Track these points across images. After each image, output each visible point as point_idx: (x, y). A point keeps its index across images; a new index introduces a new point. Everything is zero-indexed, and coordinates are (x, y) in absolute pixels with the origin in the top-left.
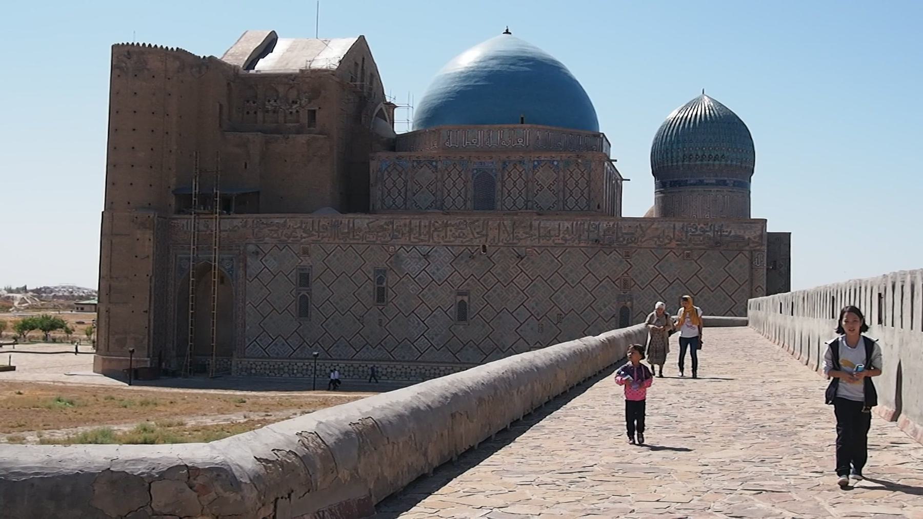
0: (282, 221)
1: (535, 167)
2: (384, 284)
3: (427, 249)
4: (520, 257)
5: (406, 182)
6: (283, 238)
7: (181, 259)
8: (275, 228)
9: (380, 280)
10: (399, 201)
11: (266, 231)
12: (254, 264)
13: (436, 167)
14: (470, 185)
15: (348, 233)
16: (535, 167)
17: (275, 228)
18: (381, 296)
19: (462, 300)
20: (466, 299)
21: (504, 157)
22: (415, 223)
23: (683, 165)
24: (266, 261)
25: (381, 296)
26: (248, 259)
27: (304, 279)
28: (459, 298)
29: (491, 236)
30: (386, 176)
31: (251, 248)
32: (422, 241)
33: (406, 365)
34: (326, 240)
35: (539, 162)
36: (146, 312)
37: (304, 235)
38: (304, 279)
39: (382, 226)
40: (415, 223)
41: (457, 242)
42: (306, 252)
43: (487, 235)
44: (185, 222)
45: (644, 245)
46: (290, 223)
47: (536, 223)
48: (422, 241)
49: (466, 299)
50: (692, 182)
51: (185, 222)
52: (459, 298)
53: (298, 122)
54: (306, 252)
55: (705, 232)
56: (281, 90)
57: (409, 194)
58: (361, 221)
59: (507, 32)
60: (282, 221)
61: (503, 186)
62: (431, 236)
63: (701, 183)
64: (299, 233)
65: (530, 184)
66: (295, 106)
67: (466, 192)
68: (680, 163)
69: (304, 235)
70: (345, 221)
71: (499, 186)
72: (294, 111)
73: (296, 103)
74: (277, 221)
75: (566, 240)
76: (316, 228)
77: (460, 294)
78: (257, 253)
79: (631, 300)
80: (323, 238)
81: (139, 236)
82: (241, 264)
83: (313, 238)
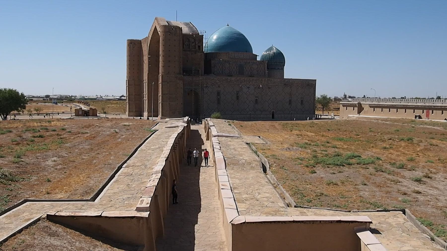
0: (213, 78)
1: (253, 64)
2: (238, 95)
3: (249, 86)
4: (269, 88)
6: (213, 83)
8: (211, 80)
9: (237, 94)
13: (230, 63)
14: (238, 68)
15: (230, 82)
17: (211, 80)
18: (238, 98)
19: (256, 99)
20: (257, 98)
21: (246, 61)
23: (275, 64)
25: (238, 98)
27: (219, 94)
28: (256, 98)
29: (263, 83)
30: (217, 65)
31: (205, 85)
32: (247, 84)
33: (244, 115)
35: (254, 63)
36: (182, 104)
38: (219, 94)
39: (238, 80)
40: (246, 79)
41: (256, 84)
42: (219, 87)
43: (262, 83)
44: (186, 78)
46: (215, 79)
48: (247, 84)
49: (257, 98)
50: (276, 68)
52: (256, 98)
53: (195, 49)
54: (219, 87)
57: (223, 70)
59: (228, 25)
60: (213, 78)
61: (246, 69)
62: (250, 83)
63: (278, 69)
64: (217, 81)
65: (252, 68)
66: (193, 44)
67: (237, 70)
70: (229, 78)
71: (245, 68)
72: (193, 45)
73: (193, 43)
74: (212, 78)
75: (278, 84)
76: (222, 80)
77: (256, 97)
78: (206, 87)
79: (292, 98)
81: (178, 82)
82: (202, 90)
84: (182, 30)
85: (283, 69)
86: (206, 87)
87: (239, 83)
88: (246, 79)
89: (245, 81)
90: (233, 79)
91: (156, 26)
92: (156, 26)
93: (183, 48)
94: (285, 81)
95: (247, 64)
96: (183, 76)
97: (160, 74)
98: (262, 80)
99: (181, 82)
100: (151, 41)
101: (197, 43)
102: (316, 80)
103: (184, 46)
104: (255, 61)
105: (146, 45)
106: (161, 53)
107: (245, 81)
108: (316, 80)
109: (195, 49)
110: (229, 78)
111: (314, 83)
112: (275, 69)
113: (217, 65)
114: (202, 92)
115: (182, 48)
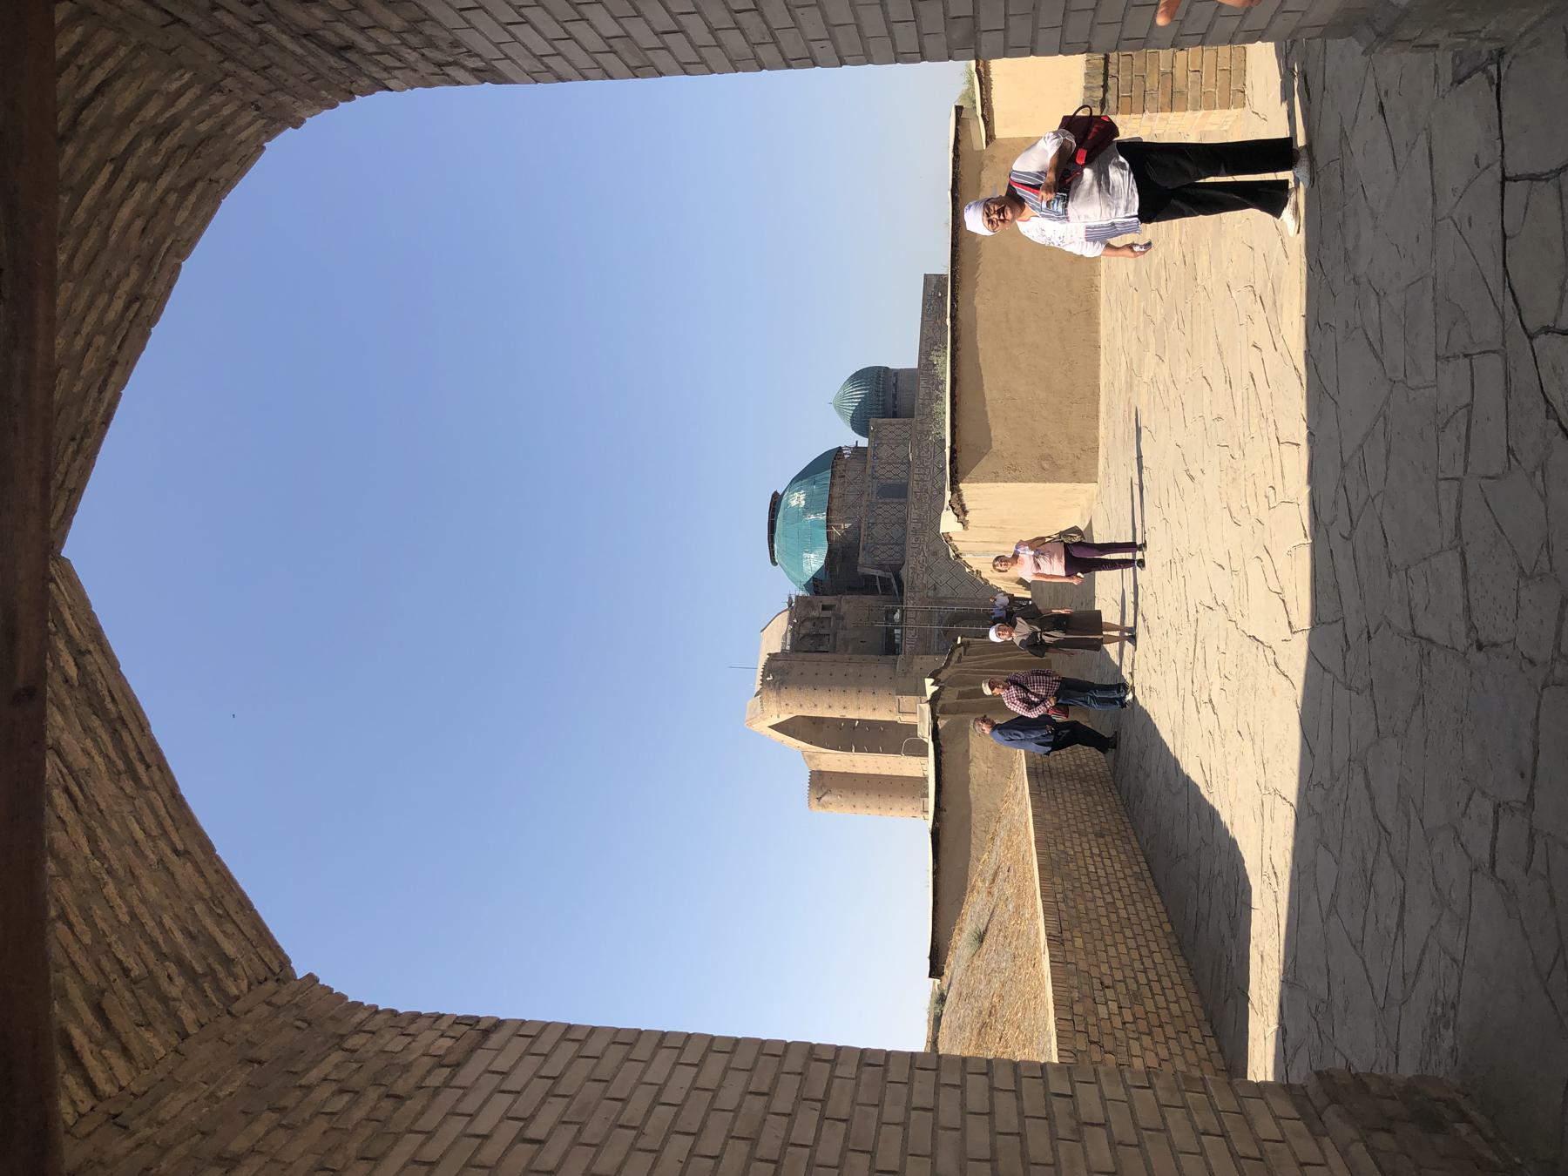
0: (911, 571)
1: (878, 458)
5: (883, 545)
7: (938, 649)
10: (897, 548)
11: (918, 582)
12: (944, 592)
13: (873, 524)
14: (888, 500)
15: (922, 523)
16: (878, 458)
22: (916, 477)
24: (941, 582)
26: (940, 595)
30: (877, 558)
31: (931, 593)
34: (926, 539)
37: (922, 554)
42: (935, 554)
44: (908, 646)
45: (938, 337)
47: (921, 401)
51: (908, 646)
53: (830, 618)
55: (931, 305)
56: (803, 632)
57: (891, 542)
58: (914, 486)
60: (911, 571)
68: (881, 399)
69: (922, 554)
75: (933, 383)
78: (935, 589)
80: (924, 540)
83: (925, 548)
84: (776, 654)
85: (897, 373)
86: (935, 589)
87: (927, 495)
88: (916, 477)
89: (922, 480)
90: (914, 514)
91: (770, 727)
92: (770, 727)
93: (827, 652)
94: (925, 365)
95: (877, 475)
96: (902, 656)
97: (895, 720)
98: (921, 432)
99: (918, 660)
100: (811, 743)
101: (814, 614)
102: (925, 275)
103: (822, 648)
104: (870, 452)
105: (823, 756)
106: (836, 713)
107: (922, 480)
108: (925, 275)
109: (830, 618)
110: (911, 526)
111: (934, 281)
112: (895, 396)
113: (877, 558)
114: (950, 601)
115: (824, 656)
